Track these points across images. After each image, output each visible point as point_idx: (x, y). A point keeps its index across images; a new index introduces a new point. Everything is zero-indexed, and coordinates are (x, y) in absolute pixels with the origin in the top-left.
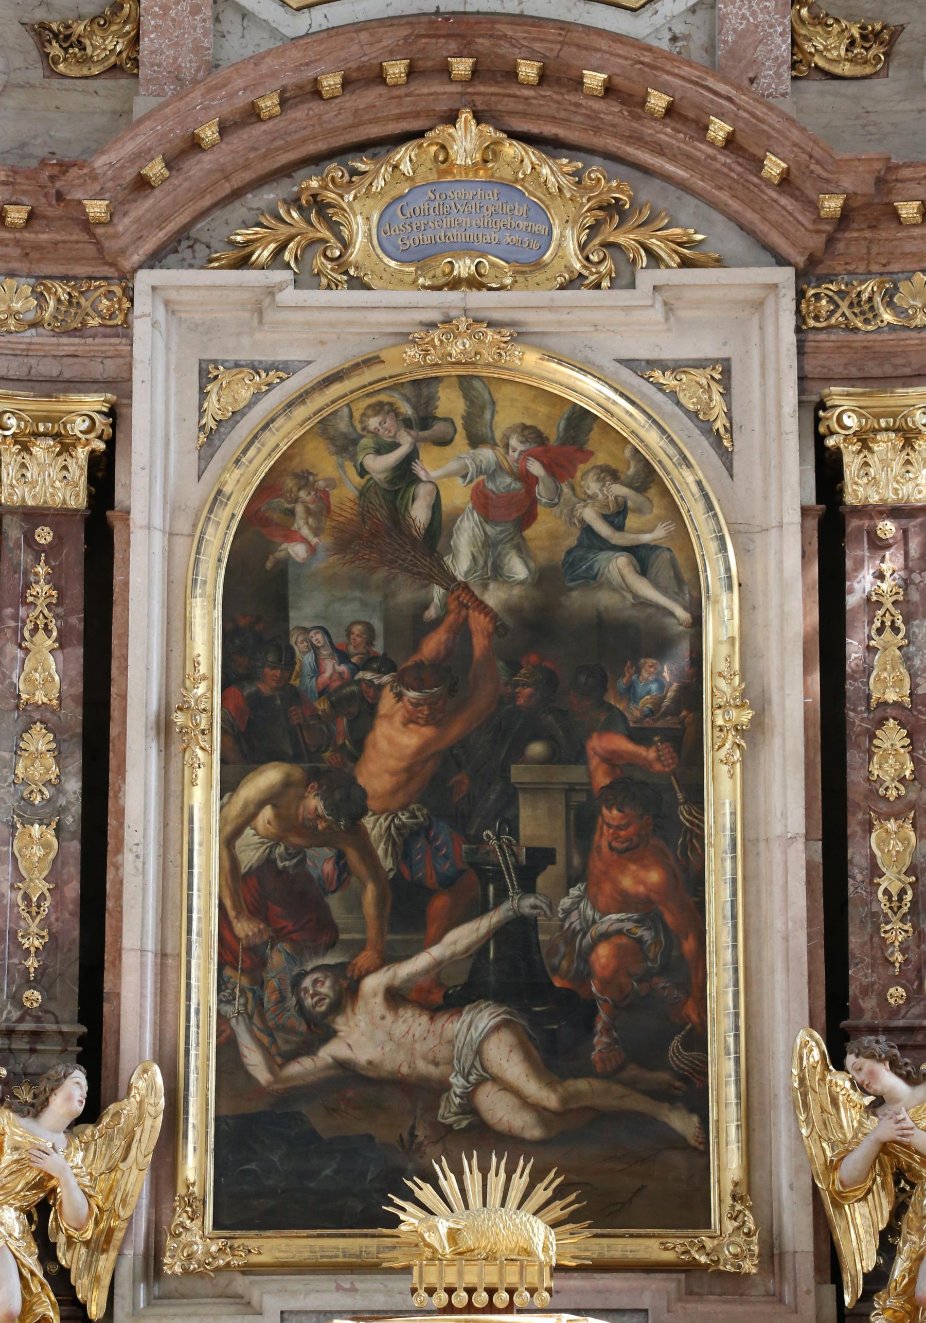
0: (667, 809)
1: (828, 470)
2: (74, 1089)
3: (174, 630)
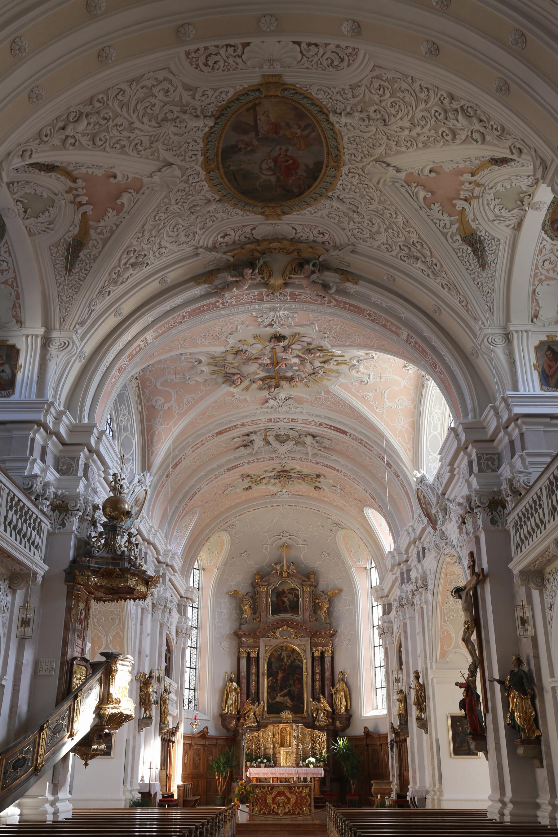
0: (300, 681)
1: (313, 653)
2: (257, 704)
3: (264, 667)
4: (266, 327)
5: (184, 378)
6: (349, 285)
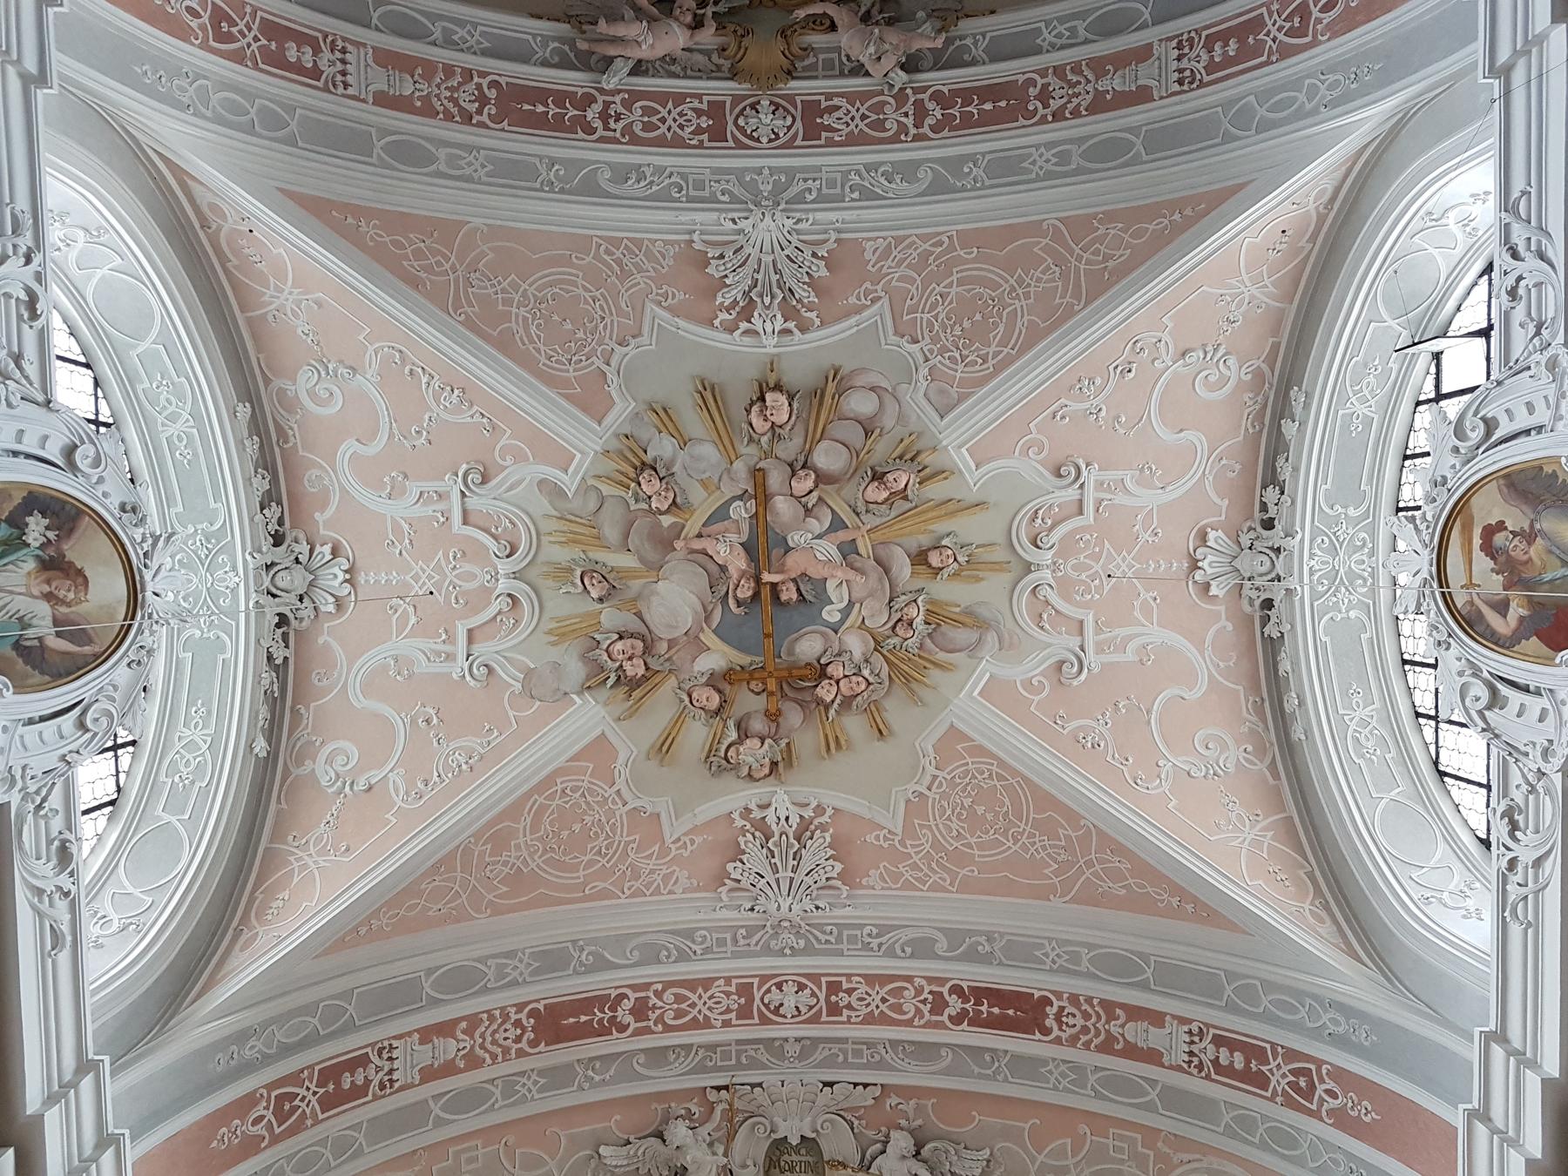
4: (730, 329)
5: (450, 657)
6: (966, 26)
